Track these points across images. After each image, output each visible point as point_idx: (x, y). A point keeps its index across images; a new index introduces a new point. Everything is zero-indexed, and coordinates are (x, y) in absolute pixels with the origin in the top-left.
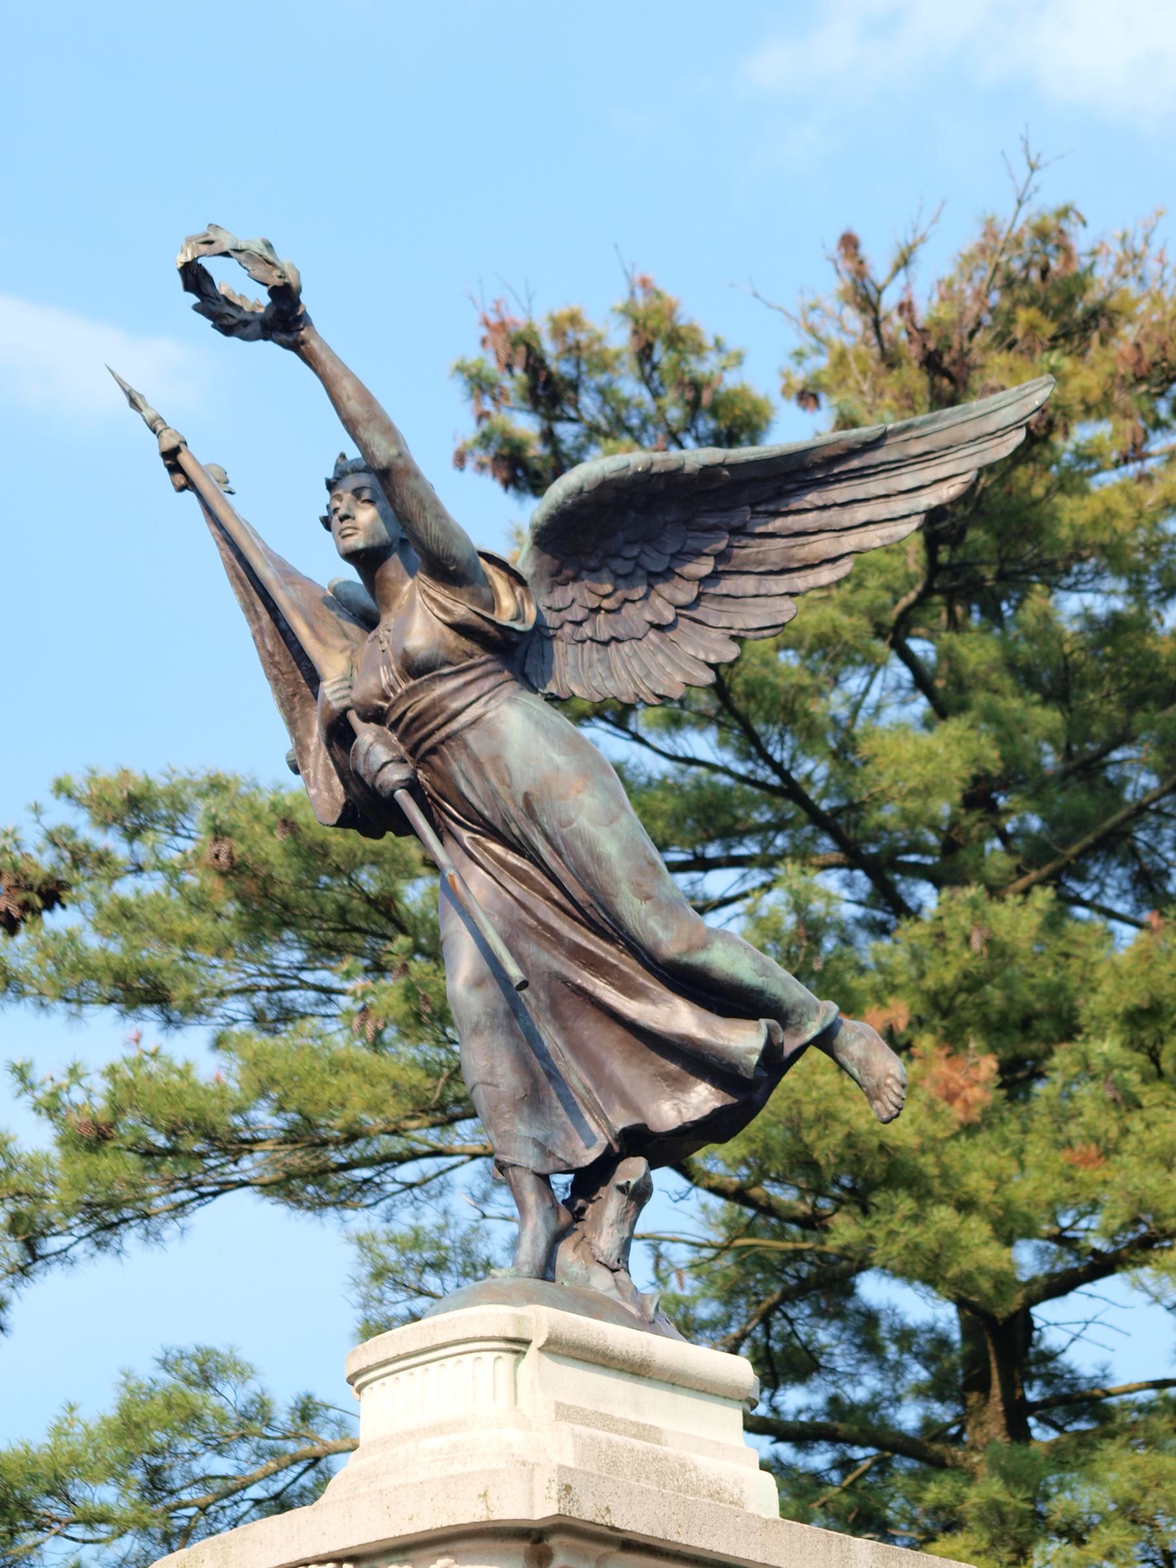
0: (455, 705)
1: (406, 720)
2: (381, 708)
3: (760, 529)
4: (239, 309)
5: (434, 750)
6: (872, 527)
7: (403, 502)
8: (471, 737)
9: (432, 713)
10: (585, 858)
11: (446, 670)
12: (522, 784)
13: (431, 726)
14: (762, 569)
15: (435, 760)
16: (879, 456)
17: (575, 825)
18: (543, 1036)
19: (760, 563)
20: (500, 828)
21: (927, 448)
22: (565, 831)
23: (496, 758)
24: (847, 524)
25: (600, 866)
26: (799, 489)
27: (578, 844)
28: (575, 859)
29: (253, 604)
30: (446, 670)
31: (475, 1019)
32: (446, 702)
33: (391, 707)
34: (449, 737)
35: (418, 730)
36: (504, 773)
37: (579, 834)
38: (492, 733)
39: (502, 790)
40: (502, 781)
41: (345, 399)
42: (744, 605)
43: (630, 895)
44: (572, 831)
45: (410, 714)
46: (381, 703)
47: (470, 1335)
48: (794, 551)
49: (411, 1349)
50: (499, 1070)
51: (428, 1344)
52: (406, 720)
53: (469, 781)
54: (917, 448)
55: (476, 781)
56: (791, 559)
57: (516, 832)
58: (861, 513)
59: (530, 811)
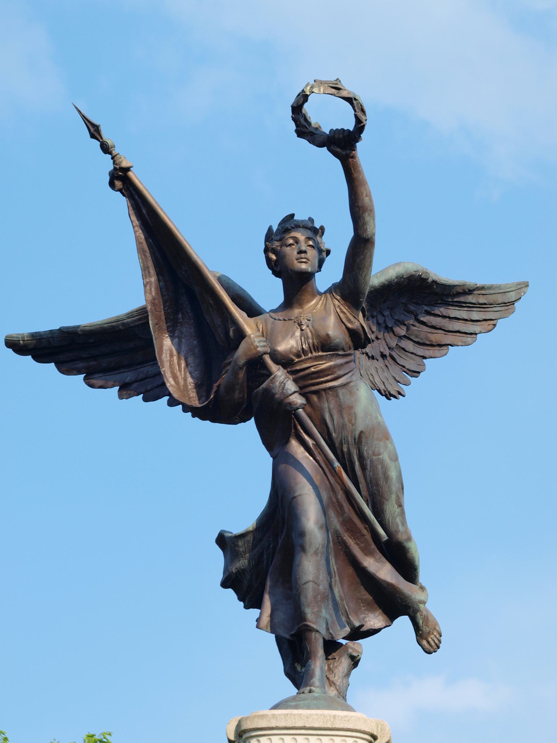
0: (341, 372)
1: (307, 372)
2: (293, 360)
3: (422, 319)
4: (309, 124)
5: (316, 392)
6: (458, 334)
7: (364, 259)
8: (341, 392)
9: (327, 373)
10: (381, 475)
11: (341, 353)
12: (360, 426)
13: (323, 379)
14: (416, 340)
15: (315, 398)
16: (470, 299)
17: (381, 456)
18: (331, 562)
19: (417, 336)
20: (337, 445)
21: (485, 301)
22: (374, 457)
23: (351, 408)
24: (451, 329)
25: (386, 482)
26: (441, 303)
27: (380, 467)
28: (374, 474)
29: (148, 268)
30: (341, 353)
31: (317, 546)
32: (335, 370)
33: (298, 362)
34: (330, 388)
35: (312, 379)
36: (353, 417)
37: (382, 462)
38: (351, 393)
39: (349, 426)
40: (350, 421)
41: (364, 195)
42: (407, 356)
43: (394, 502)
44: (378, 459)
45: (312, 369)
46: (294, 358)
47: (358, 728)
48: (429, 335)
49: (316, 725)
50: (321, 578)
51: (329, 725)
52: (307, 372)
53: (331, 416)
54: (482, 300)
55: (335, 417)
56: (427, 338)
57: (345, 450)
58: (457, 326)
59: (359, 441)
